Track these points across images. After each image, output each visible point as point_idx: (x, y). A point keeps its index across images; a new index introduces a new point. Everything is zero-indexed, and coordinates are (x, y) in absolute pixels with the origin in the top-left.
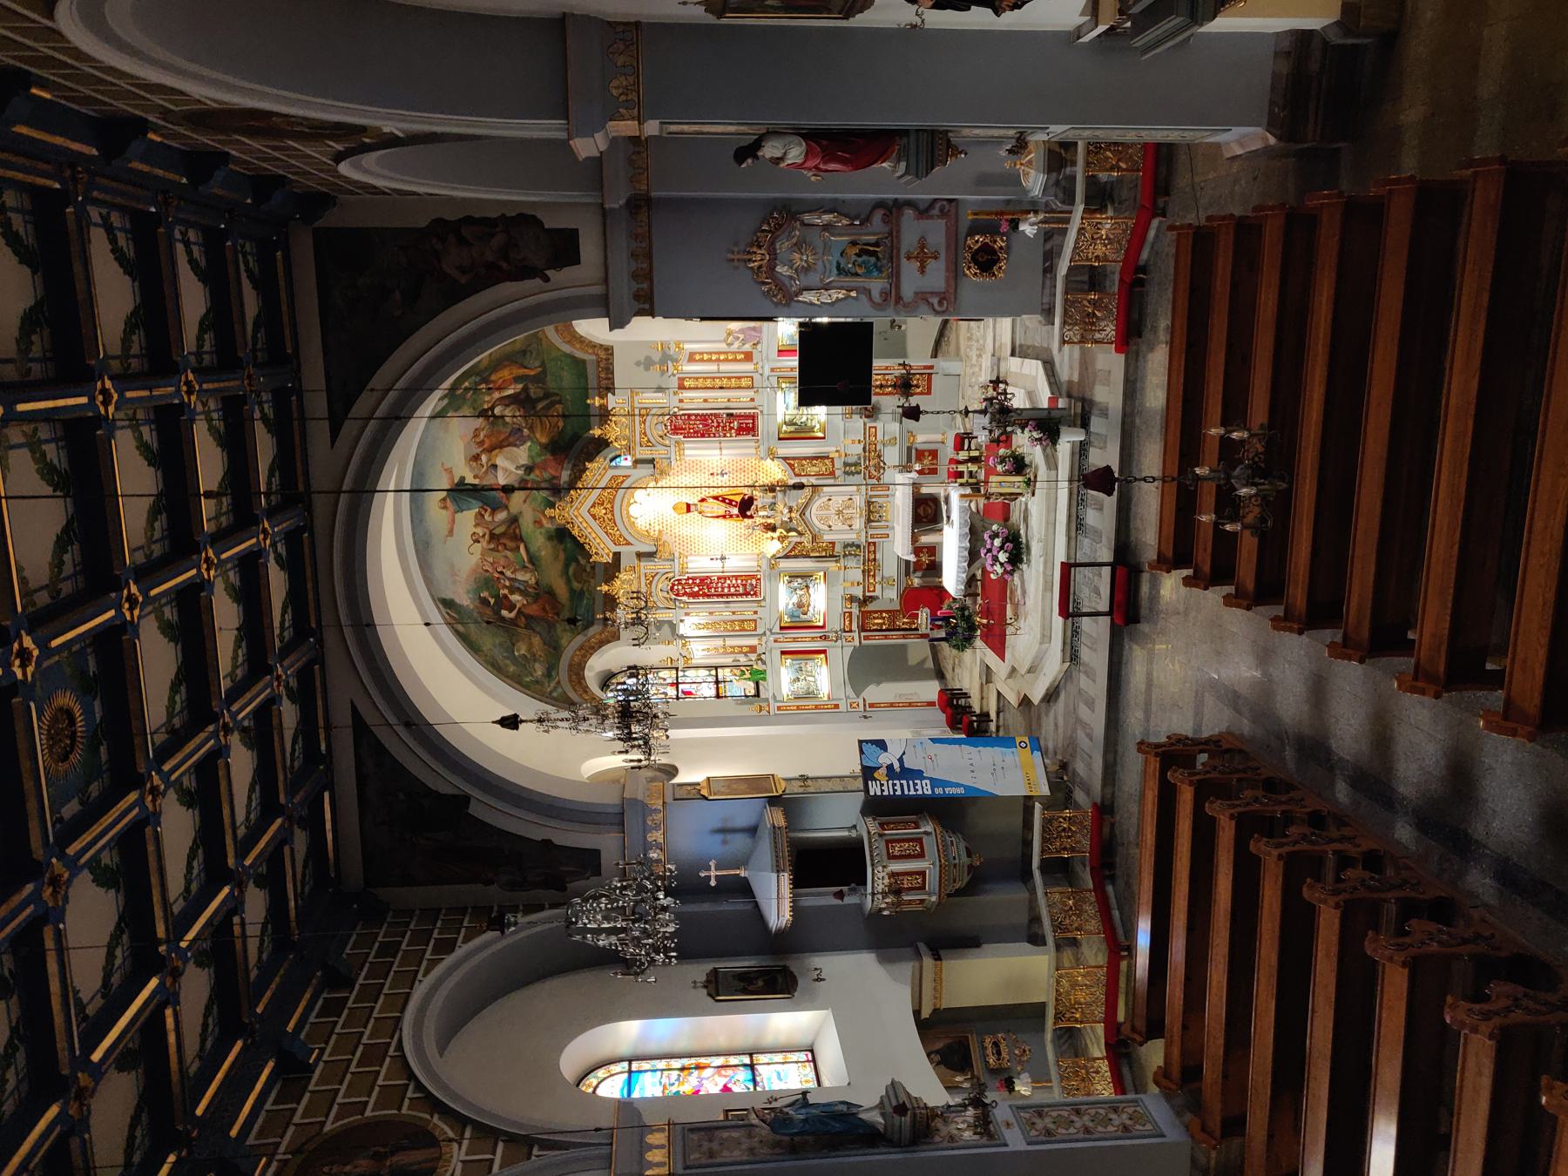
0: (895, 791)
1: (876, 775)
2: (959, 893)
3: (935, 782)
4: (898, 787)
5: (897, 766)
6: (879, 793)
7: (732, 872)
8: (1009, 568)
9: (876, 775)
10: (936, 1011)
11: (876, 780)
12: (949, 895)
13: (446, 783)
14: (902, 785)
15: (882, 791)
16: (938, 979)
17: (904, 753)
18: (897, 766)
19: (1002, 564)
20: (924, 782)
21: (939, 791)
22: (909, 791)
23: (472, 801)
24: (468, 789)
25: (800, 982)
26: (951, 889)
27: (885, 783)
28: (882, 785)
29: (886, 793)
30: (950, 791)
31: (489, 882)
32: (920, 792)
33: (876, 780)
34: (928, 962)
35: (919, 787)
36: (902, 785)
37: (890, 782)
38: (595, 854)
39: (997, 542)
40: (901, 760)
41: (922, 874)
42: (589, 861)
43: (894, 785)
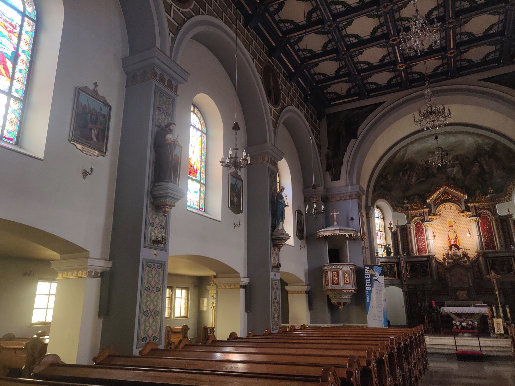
0: (367, 276)
1: (371, 270)
2: (329, 300)
3: (370, 291)
4: (367, 277)
5: (375, 278)
6: (366, 270)
7: (335, 220)
8: (460, 327)
9: (371, 270)
10: (287, 292)
11: (370, 269)
12: (328, 296)
13: (362, 130)
14: (369, 279)
15: (366, 271)
16: (299, 292)
17: (379, 282)
18: (375, 278)
19: (461, 324)
20: (370, 287)
21: (367, 292)
22: (367, 281)
23: (356, 140)
24: (359, 139)
25: (300, 241)
26: (331, 296)
27: (369, 273)
28: (368, 271)
29: (366, 272)
30: (368, 296)
31: (328, 148)
32: (367, 285)
33: (370, 269)
34: (305, 288)
35: (368, 285)
36: (369, 279)
37: (369, 275)
38: (339, 179)
39: (470, 322)
40: (377, 280)
41: (338, 283)
42: (336, 177)
43: (368, 276)
